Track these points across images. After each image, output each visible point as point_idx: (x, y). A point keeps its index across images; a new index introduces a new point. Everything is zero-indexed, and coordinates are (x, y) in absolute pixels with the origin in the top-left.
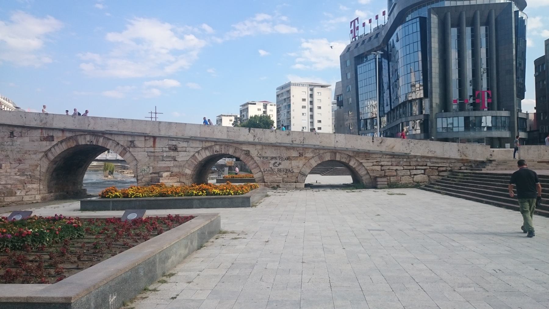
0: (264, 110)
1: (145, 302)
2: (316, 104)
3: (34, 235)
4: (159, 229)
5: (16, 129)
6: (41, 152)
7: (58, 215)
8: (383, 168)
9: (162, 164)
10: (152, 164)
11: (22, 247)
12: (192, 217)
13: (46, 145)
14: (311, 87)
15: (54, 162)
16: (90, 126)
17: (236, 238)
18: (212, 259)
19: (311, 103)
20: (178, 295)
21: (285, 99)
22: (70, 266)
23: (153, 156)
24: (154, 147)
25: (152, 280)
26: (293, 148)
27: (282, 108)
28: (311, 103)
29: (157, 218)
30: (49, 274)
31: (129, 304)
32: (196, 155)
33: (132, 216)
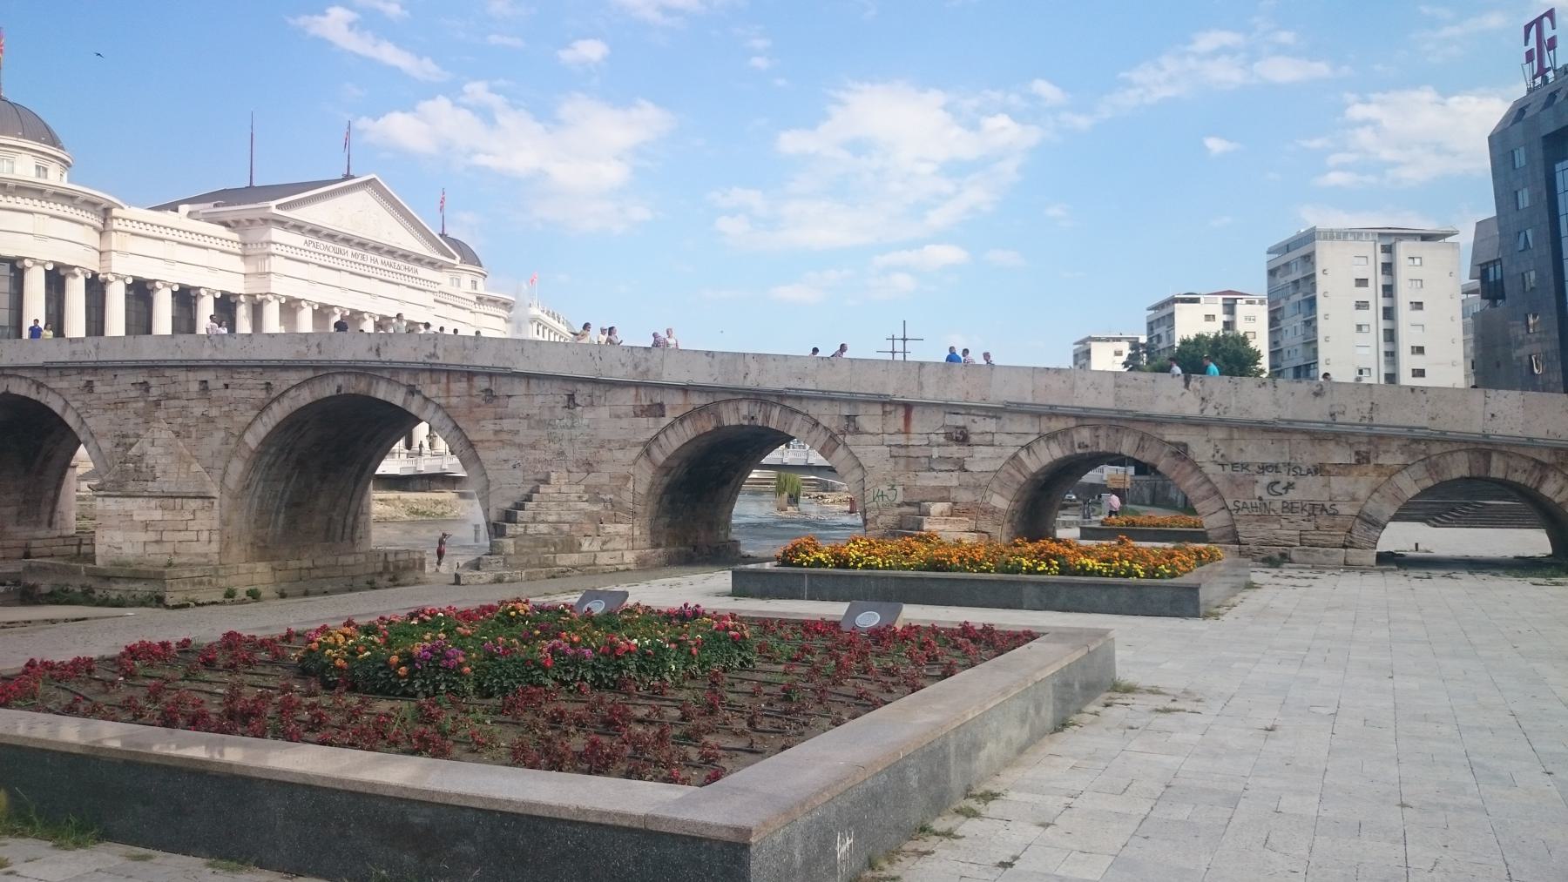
0: (1225, 318)
1: (927, 864)
2: (1404, 295)
3: (643, 655)
4: (946, 660)
5: (579, 386)
6: (635, 445)
7: (692, 605)
9: (928, 480)
10: (902, 480)
11: (615, 682)
12: (1029, 636)
14: (1387, 242)
15: (665, 469)
16: (750, 377)
17: (1167, 711)
18: (1103, 765)
19: (1389, 290)
20: (1016, 858)
21: (1296, 282)
22: (732, 743)
23: (904, 457)
24: (907, 432)
25: (939, 804)
26: (1337, 437)
27: (1288, 311)
28: (1389, 290)
29: (934, 630)
30: (685, 758)
31: (885, 864)
32: (1023, 455)
33: (869, 619)
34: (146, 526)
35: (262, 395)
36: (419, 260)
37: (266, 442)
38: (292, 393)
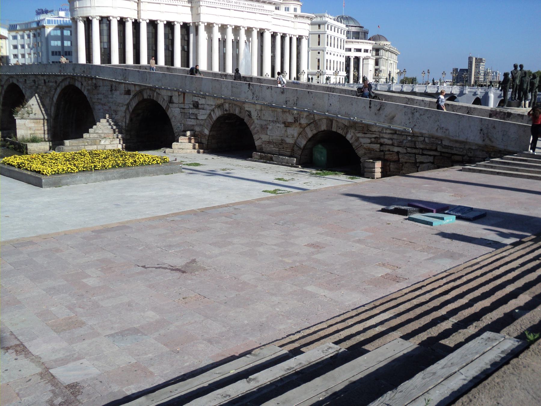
10: (183, 122)
13: (127, 98)
34: (30, 128)
35: (55, 85)
37: (59, 100)
38: (61, 84)
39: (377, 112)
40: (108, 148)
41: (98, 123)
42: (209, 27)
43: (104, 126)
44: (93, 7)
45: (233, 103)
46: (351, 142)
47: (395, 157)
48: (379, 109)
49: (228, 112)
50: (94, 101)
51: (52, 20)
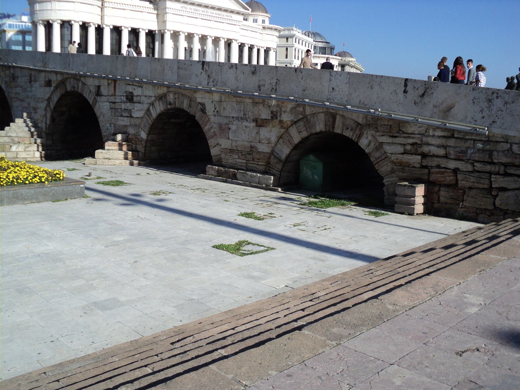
8: (428, 162)
24: (115, 95)
36: (232, 12)
39: (418, 100)
40: (21, 156)
41: (11, 124)
42: (175, 35)
43: (19, 128)
44: (54, 10)
45: (180, 91)
46: (367, 151)
47: (449, 179)
48: (423, 95)
49: (172, 106)
50: (12, 96)
51: (13, 25)
